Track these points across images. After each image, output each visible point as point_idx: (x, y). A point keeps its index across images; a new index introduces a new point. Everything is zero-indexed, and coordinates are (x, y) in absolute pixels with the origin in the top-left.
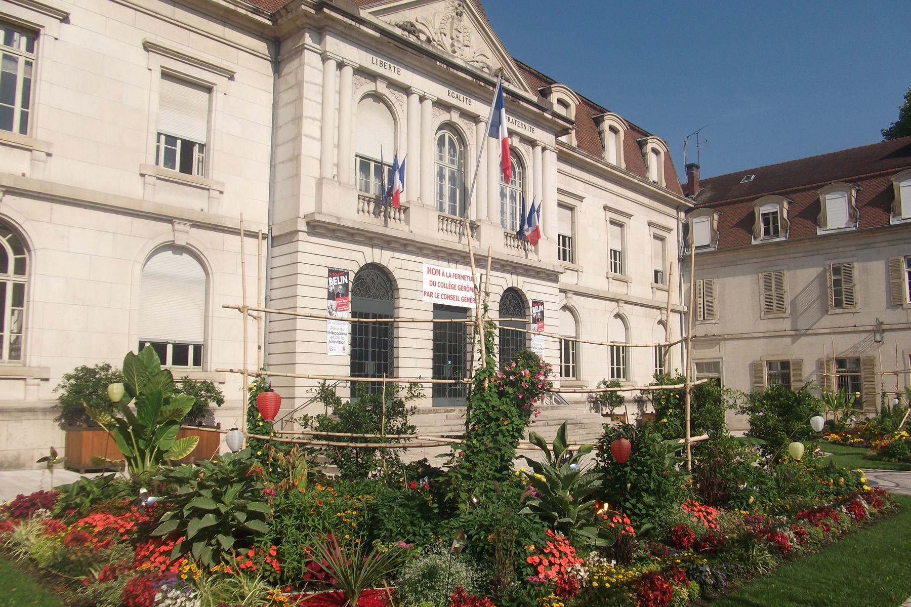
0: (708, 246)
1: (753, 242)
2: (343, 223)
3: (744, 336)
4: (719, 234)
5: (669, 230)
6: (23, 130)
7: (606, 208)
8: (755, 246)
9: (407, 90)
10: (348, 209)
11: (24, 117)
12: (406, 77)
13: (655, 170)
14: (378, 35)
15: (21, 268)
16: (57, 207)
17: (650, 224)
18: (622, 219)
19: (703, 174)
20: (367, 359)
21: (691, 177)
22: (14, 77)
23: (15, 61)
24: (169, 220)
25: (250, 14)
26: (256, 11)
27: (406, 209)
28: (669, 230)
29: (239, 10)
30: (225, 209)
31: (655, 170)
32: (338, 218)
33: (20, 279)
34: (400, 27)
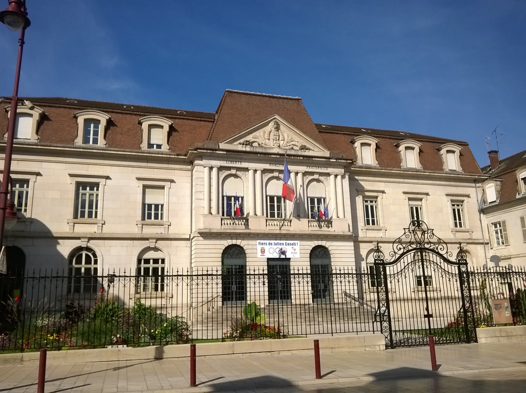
0: (495, 201)
1: (518, 197)
2: (212, 231)
3: (521, 256)
4: (501, 193)
5: (468, 196)
6: (96, 217)
7: (405, 193)
8: (518, 199)
9: (247, 170)
10: (216, 224)
11: (96, 212)
12: (244, 165)
13: (452, 162)
14: (225, 153)
15: (96, 262)
16: (107, 242)
17: (447, 195)
18: (419, 196)
19: (501, 157)
20: (232, 285)
21: (492, 159)
22: (93, 200)
23: (93, 195)
24: (147, 239)
25: (176, 157)
26: (178, 155)
27: (247, 220)
28: (468, 196)
29: (171, 156)
30: (173, 231)
31: (452, 162)
32: (210, 230)
33: (95, 266)
34: (240, 144)
